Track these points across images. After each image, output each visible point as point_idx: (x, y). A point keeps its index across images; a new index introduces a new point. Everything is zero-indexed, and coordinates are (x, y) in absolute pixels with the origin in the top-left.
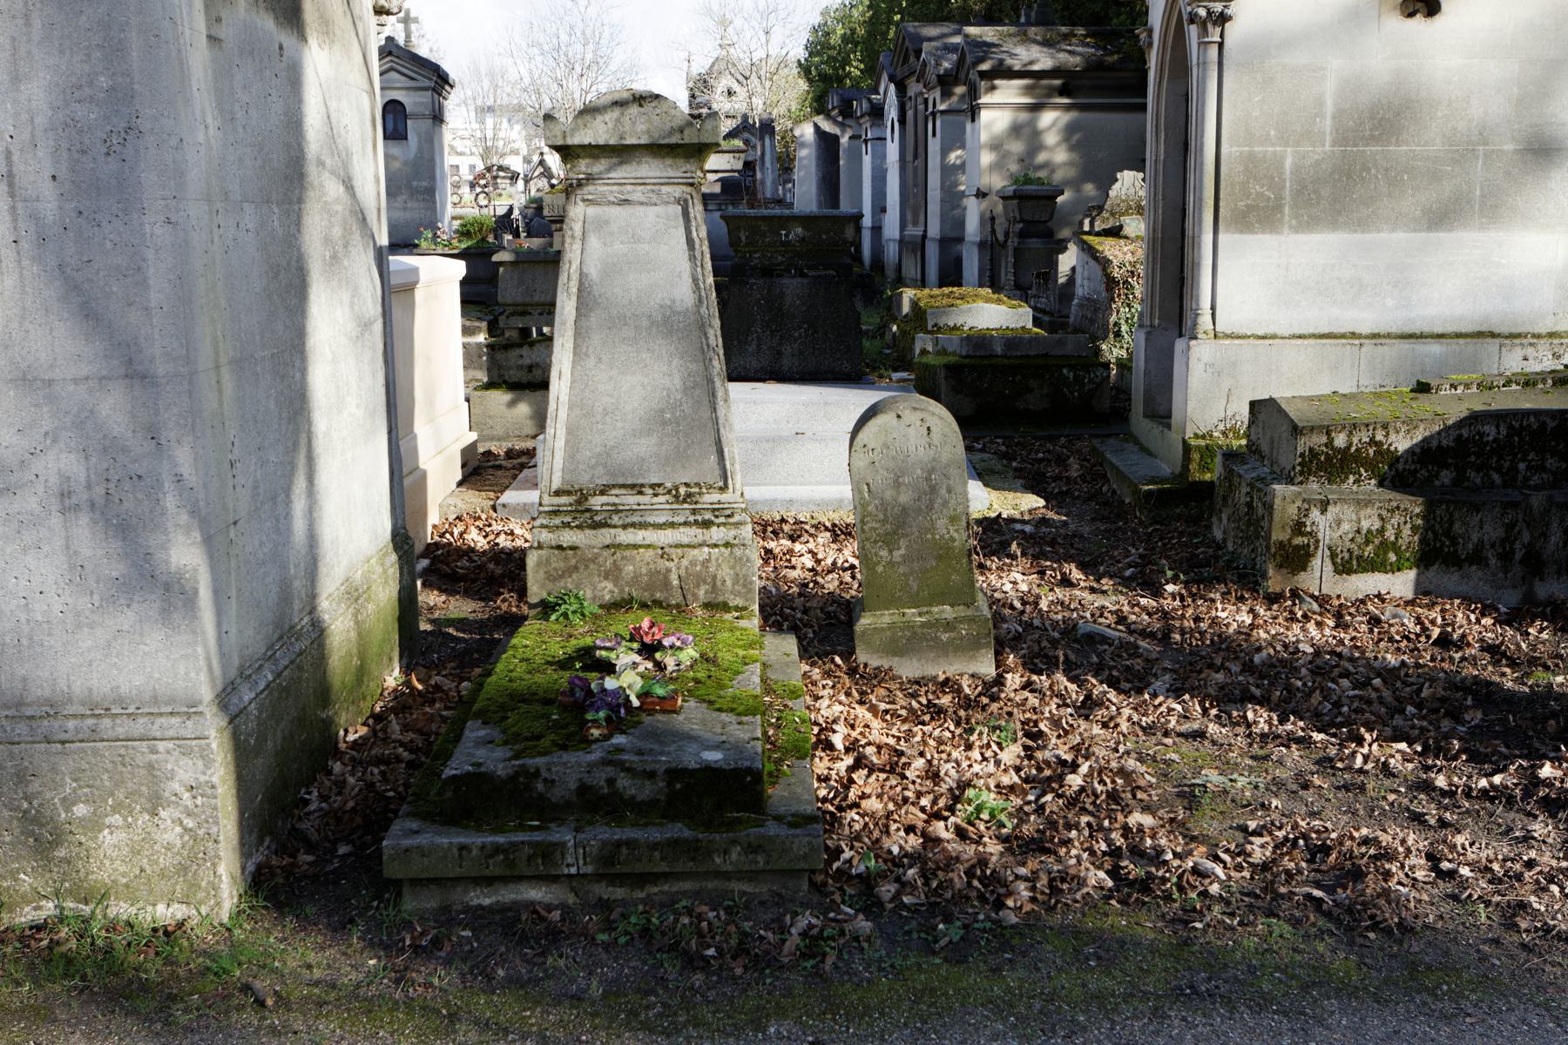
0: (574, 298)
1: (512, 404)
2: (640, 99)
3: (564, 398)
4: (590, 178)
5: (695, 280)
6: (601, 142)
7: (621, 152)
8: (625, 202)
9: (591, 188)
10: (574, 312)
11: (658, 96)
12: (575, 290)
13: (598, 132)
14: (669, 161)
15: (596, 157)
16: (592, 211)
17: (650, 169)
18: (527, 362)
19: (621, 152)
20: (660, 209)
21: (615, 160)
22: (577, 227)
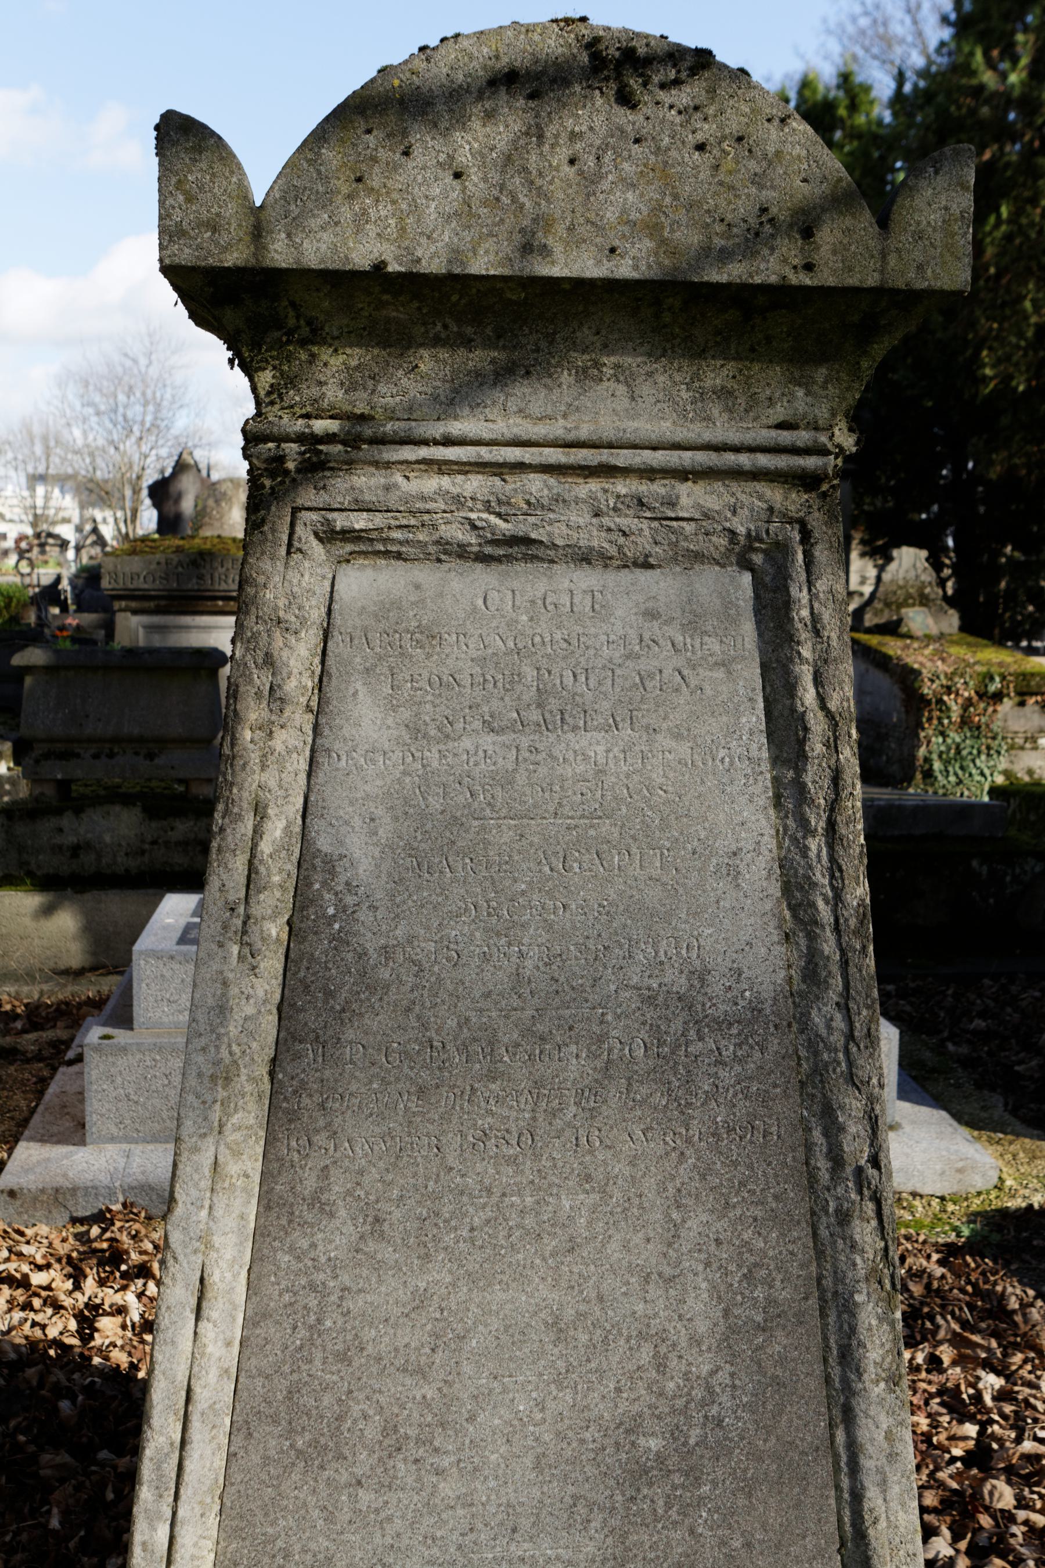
0: (272, 964)
1: (47, 911)
2: (623, 67)
3: (215, 1391)
4: (362, 438)
5: (795, 888)
6: (432, 260)
7: (511, 320)
8: (519, 549)
9: (365, 482)
10: (269, 1023)
11: (702, 60)
12: (276, 929)
13: (421, 216)
14: (717, 375)
15: (395, 340)
16: (362, 583)
17: (634, 404)
18: (71, 839)
19: (511, 320)
20: (661, 586)
21: (479, 358)
22: (298, 656)
